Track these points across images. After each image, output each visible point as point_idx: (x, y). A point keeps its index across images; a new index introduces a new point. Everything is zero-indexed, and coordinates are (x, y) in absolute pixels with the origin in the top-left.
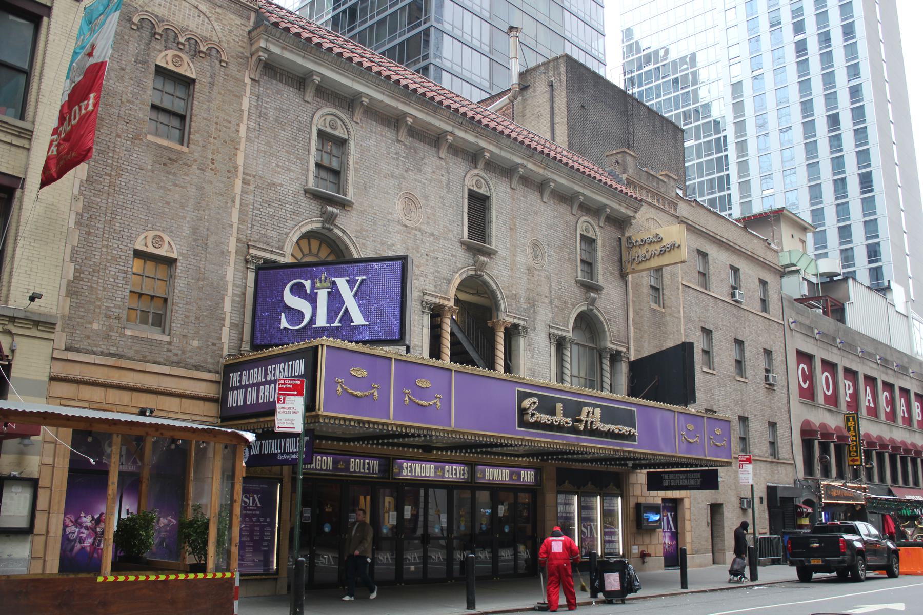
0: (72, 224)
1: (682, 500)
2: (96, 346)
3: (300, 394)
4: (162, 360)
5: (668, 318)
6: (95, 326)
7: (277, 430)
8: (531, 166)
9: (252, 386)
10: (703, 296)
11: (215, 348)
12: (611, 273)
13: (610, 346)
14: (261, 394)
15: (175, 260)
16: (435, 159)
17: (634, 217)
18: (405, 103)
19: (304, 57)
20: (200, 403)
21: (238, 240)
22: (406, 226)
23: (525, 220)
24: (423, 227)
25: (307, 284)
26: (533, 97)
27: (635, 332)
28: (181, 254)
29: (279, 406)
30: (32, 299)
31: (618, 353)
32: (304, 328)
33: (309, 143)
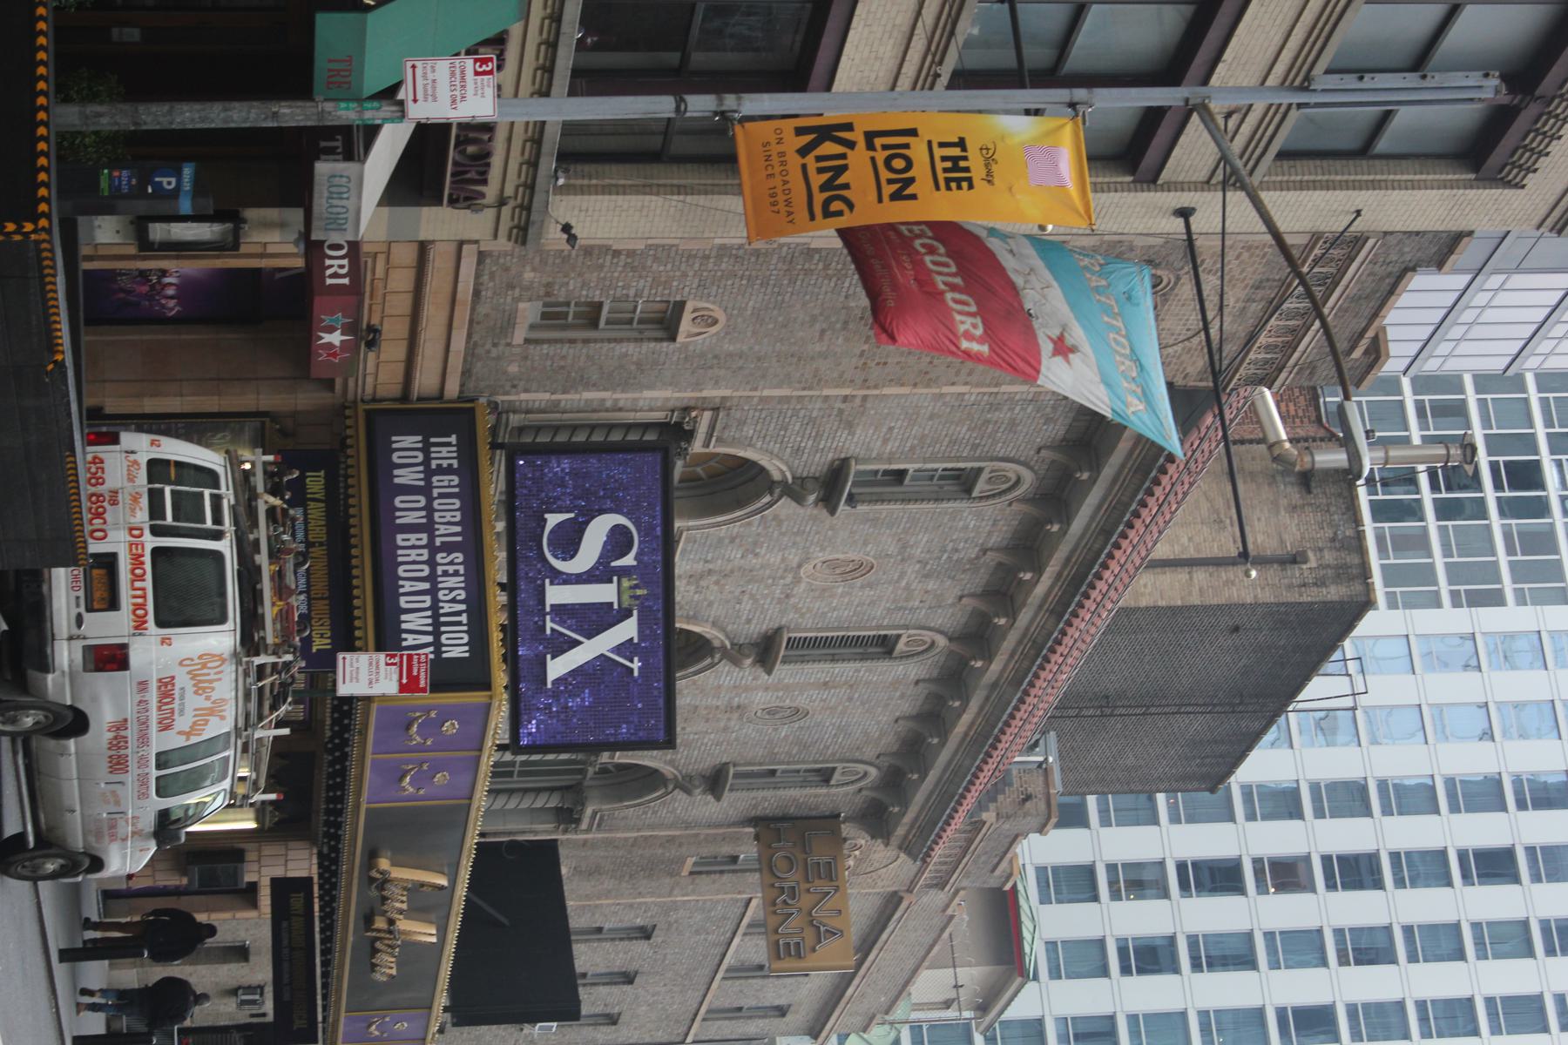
0: (718, 241)
1: (254, 904)
2: (492, 276)
3: (402, 688)
4: (476, 338)
5: (667, 880)
6: (528, 275)
7: (340, 656)
8: (966, 718)
9: (429, 509)
10: (730, 926)
11: (508, 388)
12: (755, 807)
13: (589, 811)
14: (413, 538)
15: (673, 338)
16: (957, 591)
17: (887, 845)
18: (1059, 575)
19: (1123, 466)
20: (400, 378)
21: (724, 398)
22: (800, 566)
23: (850, 699)
24: (803, 586)
25: (629, 560)
26: (1275, 503)
27: (626, 839)
28: (686, 345)
29: (382, 656)
30: (567, 228)
31: (578, 821)
32: (545, 560)
33: (950, 459)
